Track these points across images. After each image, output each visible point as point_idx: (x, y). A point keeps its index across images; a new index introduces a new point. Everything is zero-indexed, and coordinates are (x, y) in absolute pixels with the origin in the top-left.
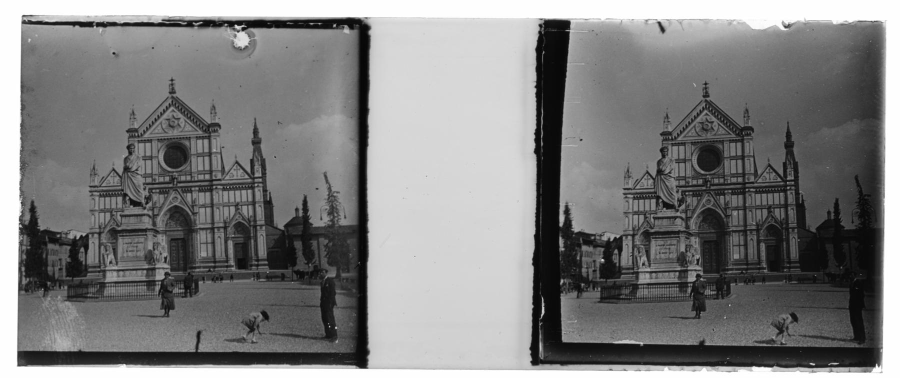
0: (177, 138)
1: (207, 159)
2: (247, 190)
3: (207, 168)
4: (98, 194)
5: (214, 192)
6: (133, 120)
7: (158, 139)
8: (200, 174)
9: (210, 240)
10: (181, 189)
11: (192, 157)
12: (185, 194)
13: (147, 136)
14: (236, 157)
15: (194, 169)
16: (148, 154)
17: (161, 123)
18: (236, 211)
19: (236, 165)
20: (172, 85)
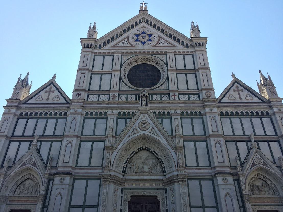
0: (149, 52)
1: (191, 78)
3: (192, 86)
4: (19, 113)
5: (208, 118)
7: (123, 53)
9: (209, 201)
10: (153, 112)
11: (170, 73)
12: (160, 120)
13: (108, 48)
14: (233, 75)
15: (173, 86)
17: (128, 37)
18: (249, 149)
19: (236, 84)
20: (143, 6)
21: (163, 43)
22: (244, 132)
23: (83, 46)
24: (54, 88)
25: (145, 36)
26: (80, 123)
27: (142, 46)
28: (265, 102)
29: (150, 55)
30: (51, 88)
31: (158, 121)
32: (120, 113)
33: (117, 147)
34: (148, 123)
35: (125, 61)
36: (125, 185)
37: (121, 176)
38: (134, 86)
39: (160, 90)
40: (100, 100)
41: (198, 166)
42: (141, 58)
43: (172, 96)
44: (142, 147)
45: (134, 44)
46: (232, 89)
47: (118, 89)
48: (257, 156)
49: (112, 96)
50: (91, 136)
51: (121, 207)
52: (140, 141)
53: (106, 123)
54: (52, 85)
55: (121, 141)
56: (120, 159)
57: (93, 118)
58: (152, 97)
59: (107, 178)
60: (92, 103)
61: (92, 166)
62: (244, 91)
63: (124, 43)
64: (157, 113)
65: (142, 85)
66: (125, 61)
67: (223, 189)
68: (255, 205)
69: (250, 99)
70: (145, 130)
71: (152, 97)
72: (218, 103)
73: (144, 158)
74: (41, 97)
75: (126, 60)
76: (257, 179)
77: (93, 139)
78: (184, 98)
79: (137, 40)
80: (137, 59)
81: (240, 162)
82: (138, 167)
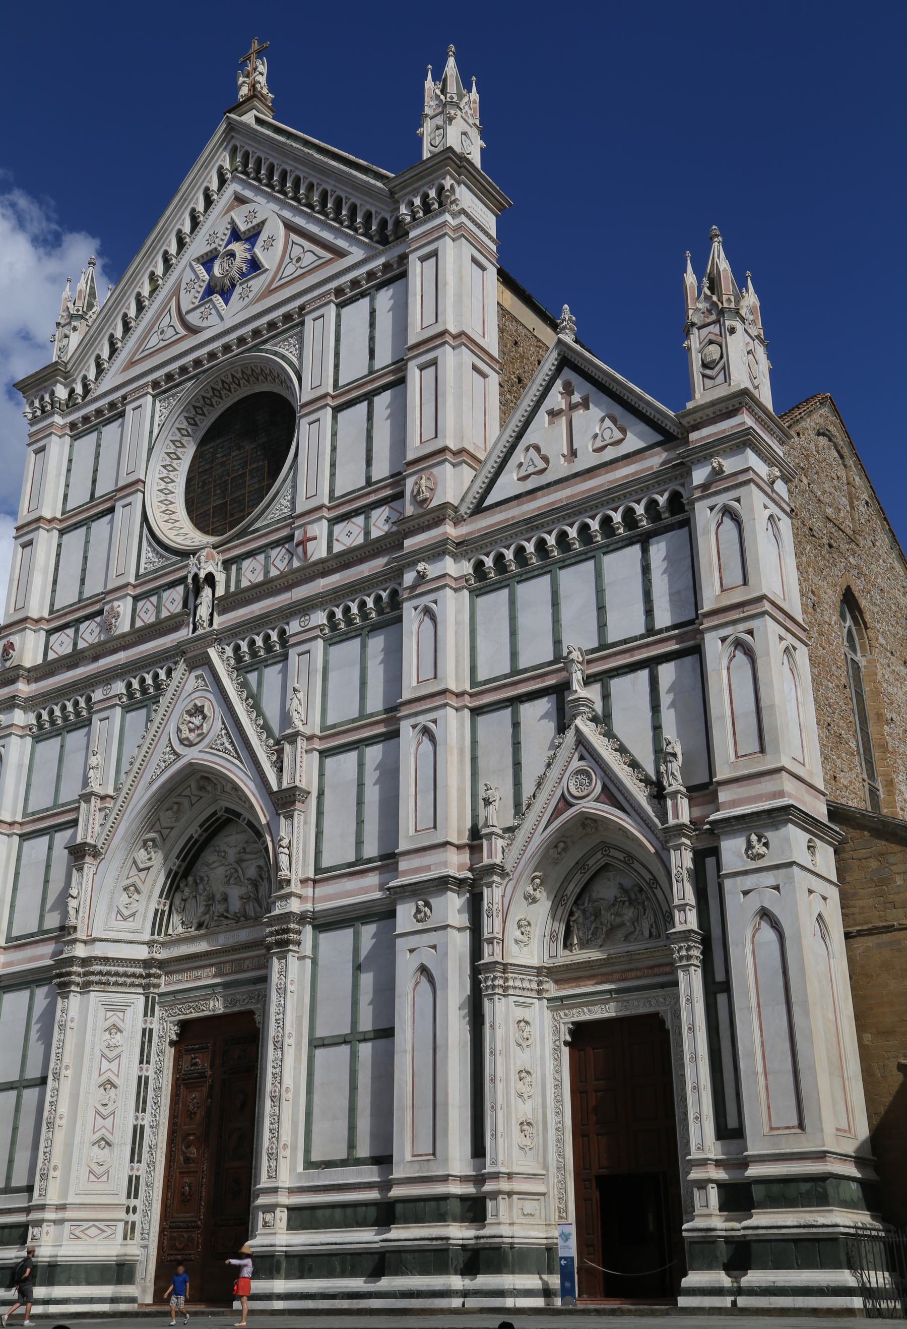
0: (241, 341)
2: (645, 540)
7: (155, 384)
8: (346, 517)
10: (229, 651)
12: (252, 677)
17: (176, 293)
19: (567, 373)
21: (299, 260)
22: (557, 643)
25: (232, 255)
26: (20, 766)
28: (676, 438)
29: (249, 350)
33: (108, 839)
34: (206, 710)
37: (142, 953)
38: (212, 535)
39: (268, 526)
41: (359, 861)
42: (223, 382)
43: (298, 545)
44: (215, 813)
45: (193, 319)
46: (542, 417)
48: (581, 758)
50: (47, 810)
51: (141, 1069)
52: (195, 792)
53: (85, 746)
56: (134, 885)
59: (69, 974)
62: (591, 405)
65: (232, 515)
67: (411, 951)
68: (562, 999)
69: (611, 444)
70: (198, 739)
71: (239, 569)
72: (472, 514)
73: (232, 854)
76: (605, 867)
78: (349, 534)
80: (206, 391)
81: (517, 805)
82: (211, 898)
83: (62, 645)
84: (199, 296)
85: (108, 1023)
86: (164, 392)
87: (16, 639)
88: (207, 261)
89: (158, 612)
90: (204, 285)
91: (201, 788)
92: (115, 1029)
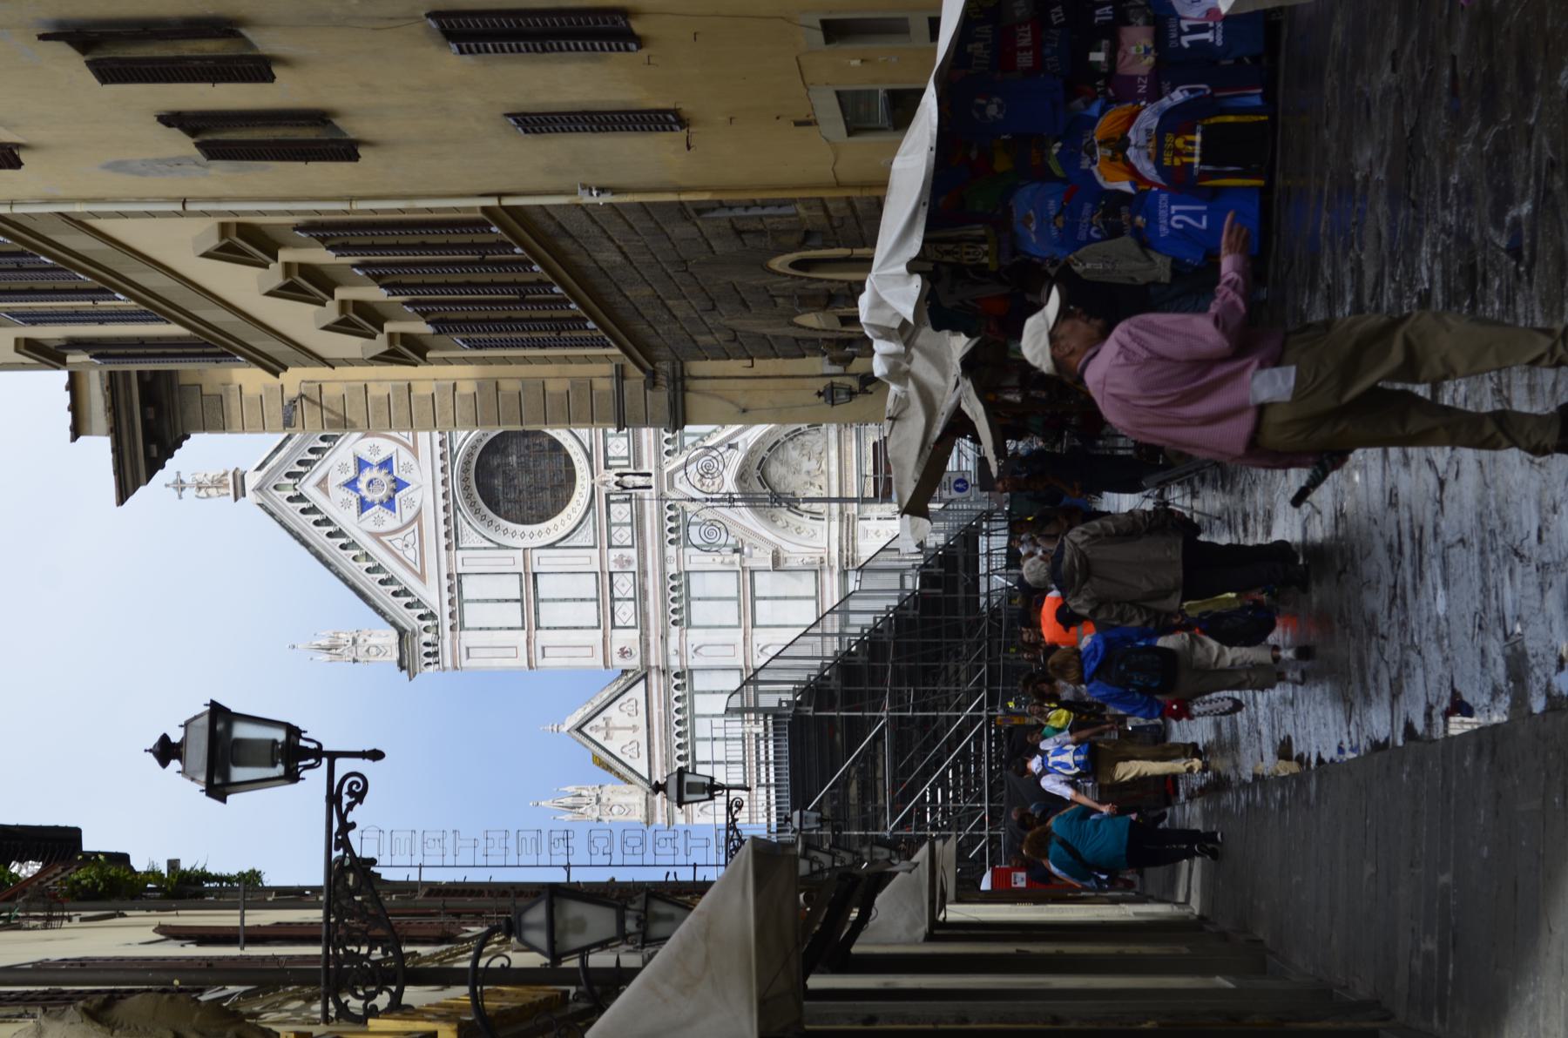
0: (443, 470)
6: (362, 651)
7: (448, 547)
10: (668, 459)
13: (432, 594)
16: (511, 588)
17: (376, 536)
23: (437, 666)
24: (598, 721)
25: (370, 482)
27: (420, 491)
30: (597, 728)
31: (694, 444)
32: (671, 542)
35: (484, 537)
36: (853, 515)
37: (835, 525)
39: (591, 437)
40: (631, 594)
44: (759, 478)
45: (408, 514)
47: (596, 552)
49: (622, 566)
50: (739, 605)
54: (586, 729)
55: (755, 534)
57: (688, 605)
58: (614, 458)
59: (847, 558)
60: (642, 615)
61: (817, 592)
63: (407, 546)
64: (670, 447)
65: (562, 480)
66: (484, 537)
71: (614, 458)
74: (630, 747)
75: (480, 533)
77: (749, 600)
79: (389, 504)
82: (806, 483)
83: (625, 613)
84: (390, 512)
85: (875, 537)
86: (457, 539)
87: (616, 648)
88: (364, 505)
89: (625, 524)
90: (382, 508)
91: (745, 482)
92: (877, 533)
